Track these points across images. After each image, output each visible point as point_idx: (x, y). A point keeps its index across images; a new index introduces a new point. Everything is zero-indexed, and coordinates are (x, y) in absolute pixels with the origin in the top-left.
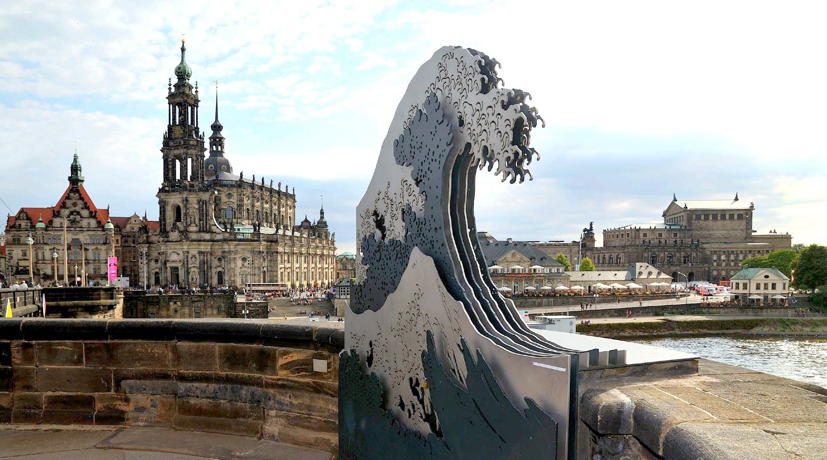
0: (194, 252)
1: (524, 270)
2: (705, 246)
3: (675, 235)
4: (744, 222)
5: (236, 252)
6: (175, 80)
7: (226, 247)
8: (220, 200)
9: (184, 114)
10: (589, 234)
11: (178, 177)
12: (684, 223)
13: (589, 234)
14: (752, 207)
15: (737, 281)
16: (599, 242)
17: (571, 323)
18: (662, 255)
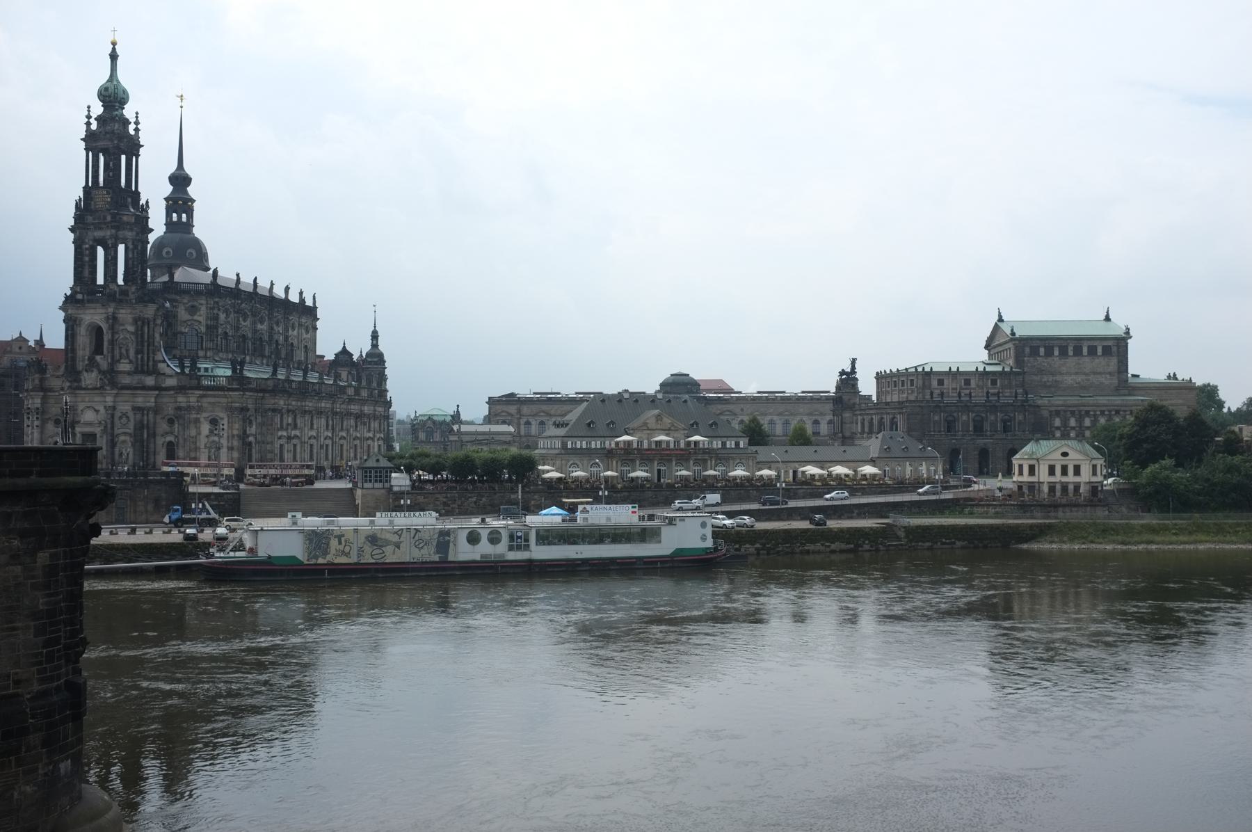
0: (124, 407)
1: (640, 442)
2: (1040, 402)
3: (994, 382)
5: (200, 409)
6: (98, 109)
7: (181, 399)
8: (175, 316)
9: (112, 170)
10: (848, 380)
11: (100, 280)
12: (1011, 362)
13: (848, 380)
14: (1128, 333)
17: (704, 525)
18: (965, 418)
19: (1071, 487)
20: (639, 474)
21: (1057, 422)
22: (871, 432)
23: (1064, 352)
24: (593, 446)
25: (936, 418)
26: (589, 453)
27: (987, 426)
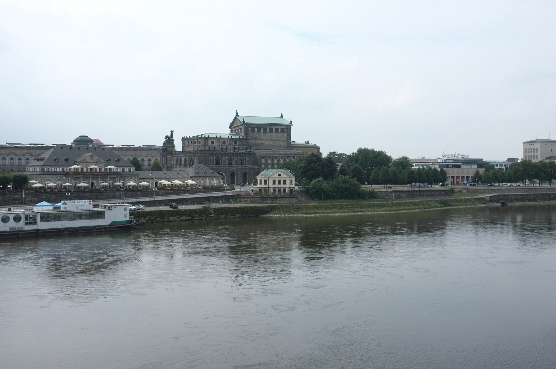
2: (256, 152)
3: (236, 143)
4: (285, 135)
10: (169, 141)
12: (243, 134)
13: (169, 141)
15: (261, 178)
16: (178, 147)
17: (125, 209)
18: (224, 159)
19: (282, 190)
20: (83, 184)
21: (263, 161)
22: (181, 164)
23: (265, 131)
24: (58, 171)
25: (212, 158)
26: (55, 174)
27: (234, 162)
